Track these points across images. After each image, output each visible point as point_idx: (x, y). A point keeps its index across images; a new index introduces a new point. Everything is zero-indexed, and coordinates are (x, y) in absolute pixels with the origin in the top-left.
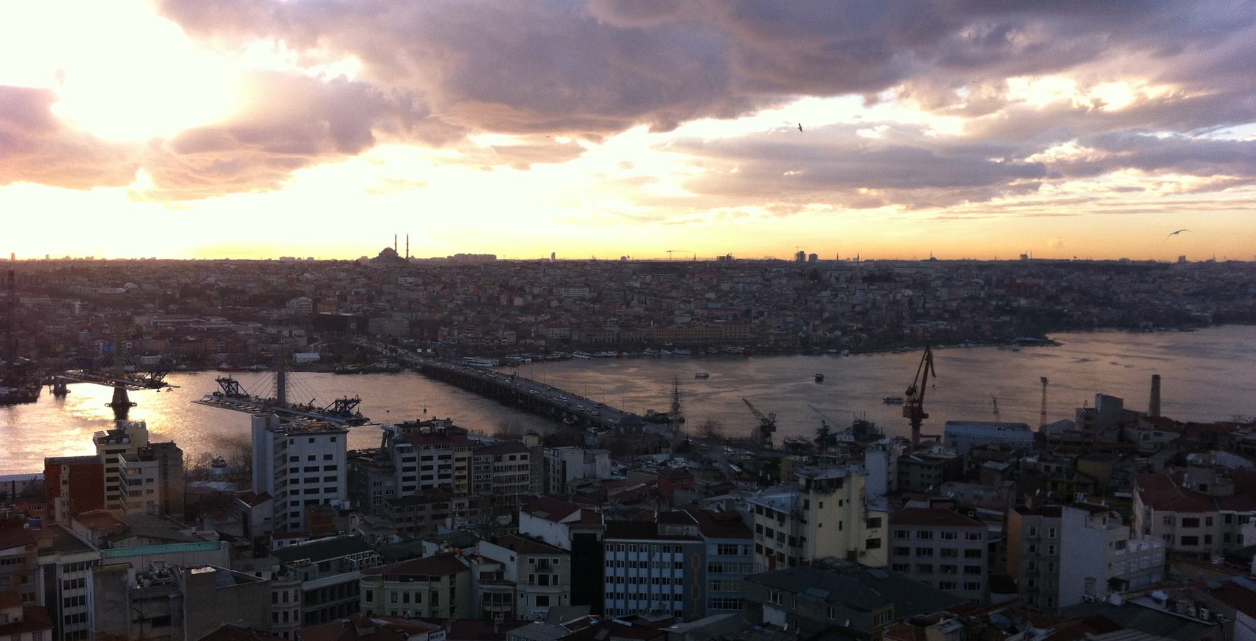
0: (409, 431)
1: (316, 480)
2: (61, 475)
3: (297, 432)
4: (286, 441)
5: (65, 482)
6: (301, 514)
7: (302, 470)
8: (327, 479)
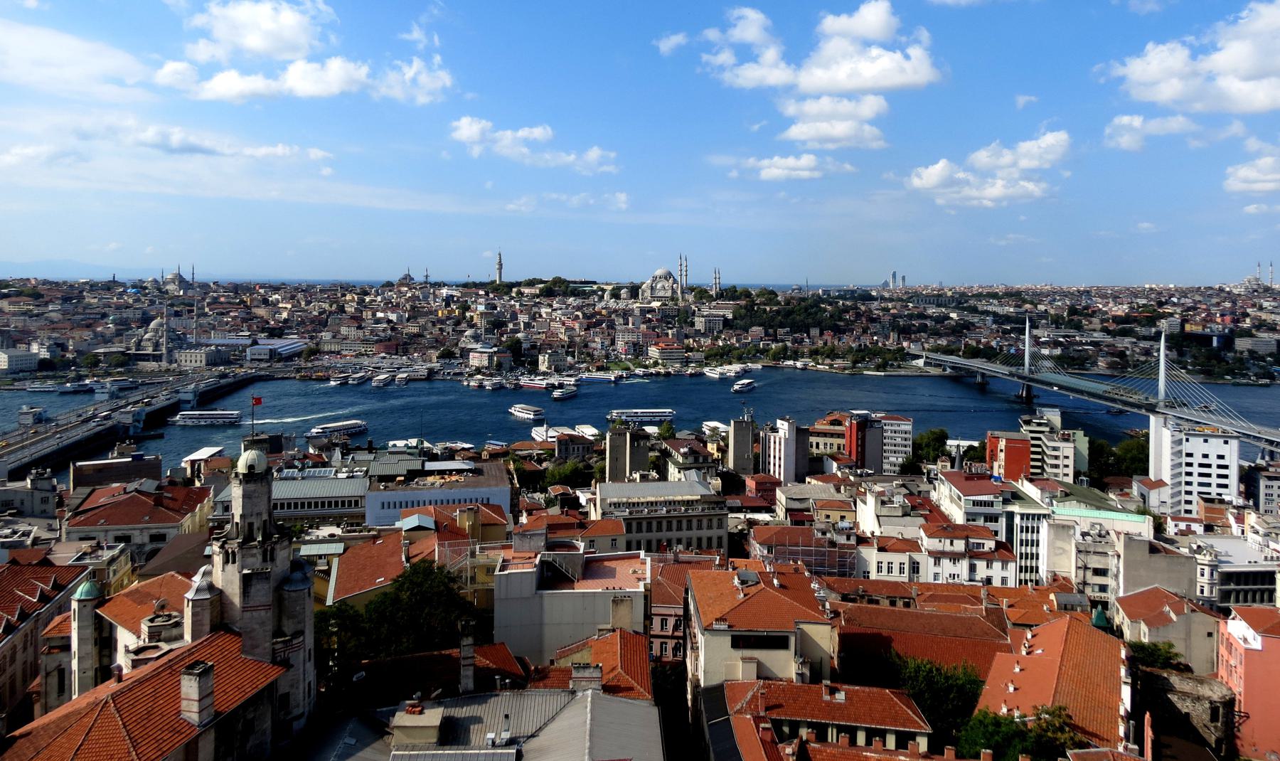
1: (1209, 475)
4: (1181, 440)
5: (1001, 451)
6: (1194, 503)
7: (1196, 465)
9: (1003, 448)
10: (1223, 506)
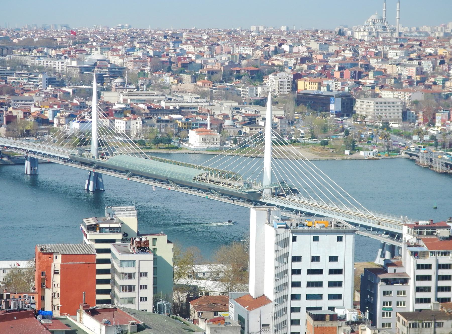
0: (420, 233)
2: (53, 265)
3: (301, 228)
4: (288, 238)
5: (56, 272)
6: (302, 322)
7: (304, 272)
8: (332, 284)
9: (58, 268)
10: (335, 324)
